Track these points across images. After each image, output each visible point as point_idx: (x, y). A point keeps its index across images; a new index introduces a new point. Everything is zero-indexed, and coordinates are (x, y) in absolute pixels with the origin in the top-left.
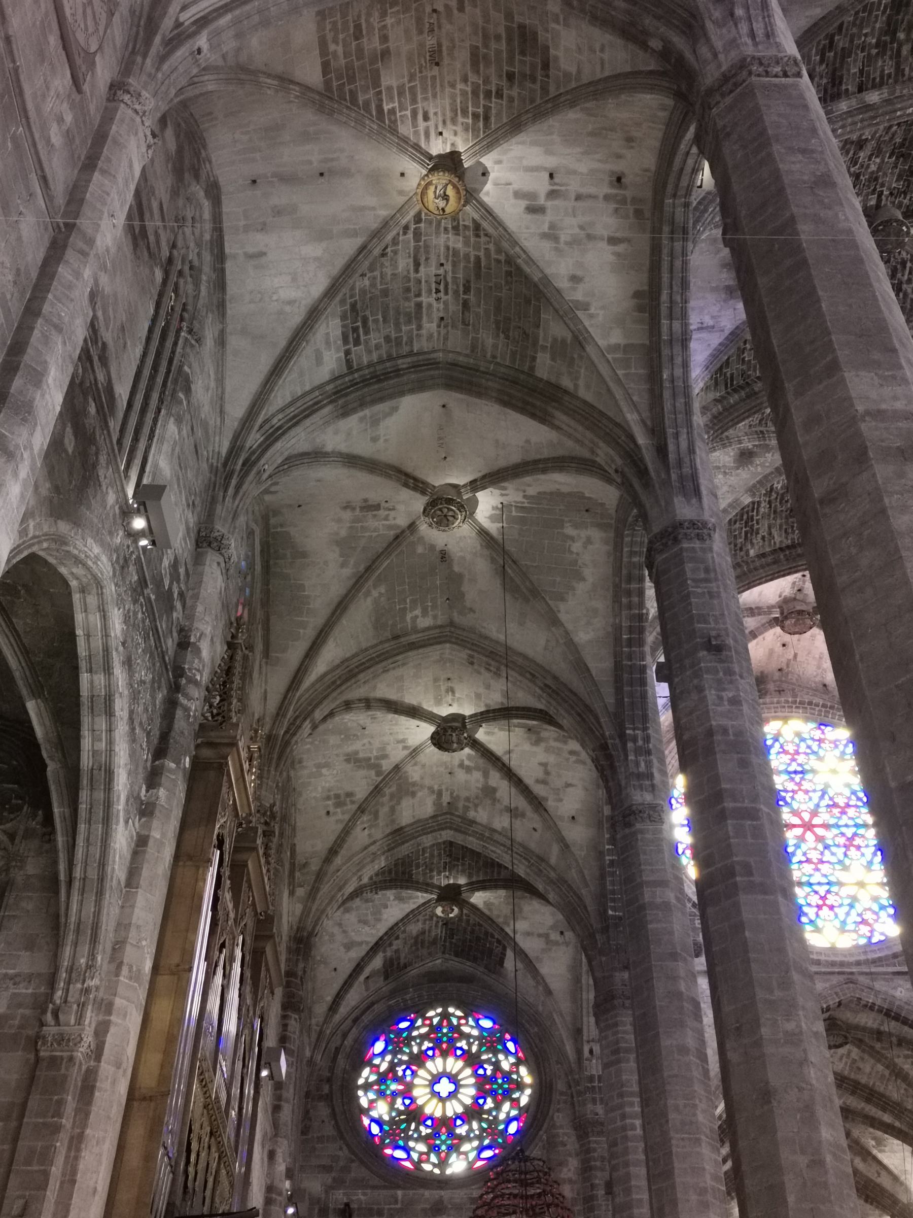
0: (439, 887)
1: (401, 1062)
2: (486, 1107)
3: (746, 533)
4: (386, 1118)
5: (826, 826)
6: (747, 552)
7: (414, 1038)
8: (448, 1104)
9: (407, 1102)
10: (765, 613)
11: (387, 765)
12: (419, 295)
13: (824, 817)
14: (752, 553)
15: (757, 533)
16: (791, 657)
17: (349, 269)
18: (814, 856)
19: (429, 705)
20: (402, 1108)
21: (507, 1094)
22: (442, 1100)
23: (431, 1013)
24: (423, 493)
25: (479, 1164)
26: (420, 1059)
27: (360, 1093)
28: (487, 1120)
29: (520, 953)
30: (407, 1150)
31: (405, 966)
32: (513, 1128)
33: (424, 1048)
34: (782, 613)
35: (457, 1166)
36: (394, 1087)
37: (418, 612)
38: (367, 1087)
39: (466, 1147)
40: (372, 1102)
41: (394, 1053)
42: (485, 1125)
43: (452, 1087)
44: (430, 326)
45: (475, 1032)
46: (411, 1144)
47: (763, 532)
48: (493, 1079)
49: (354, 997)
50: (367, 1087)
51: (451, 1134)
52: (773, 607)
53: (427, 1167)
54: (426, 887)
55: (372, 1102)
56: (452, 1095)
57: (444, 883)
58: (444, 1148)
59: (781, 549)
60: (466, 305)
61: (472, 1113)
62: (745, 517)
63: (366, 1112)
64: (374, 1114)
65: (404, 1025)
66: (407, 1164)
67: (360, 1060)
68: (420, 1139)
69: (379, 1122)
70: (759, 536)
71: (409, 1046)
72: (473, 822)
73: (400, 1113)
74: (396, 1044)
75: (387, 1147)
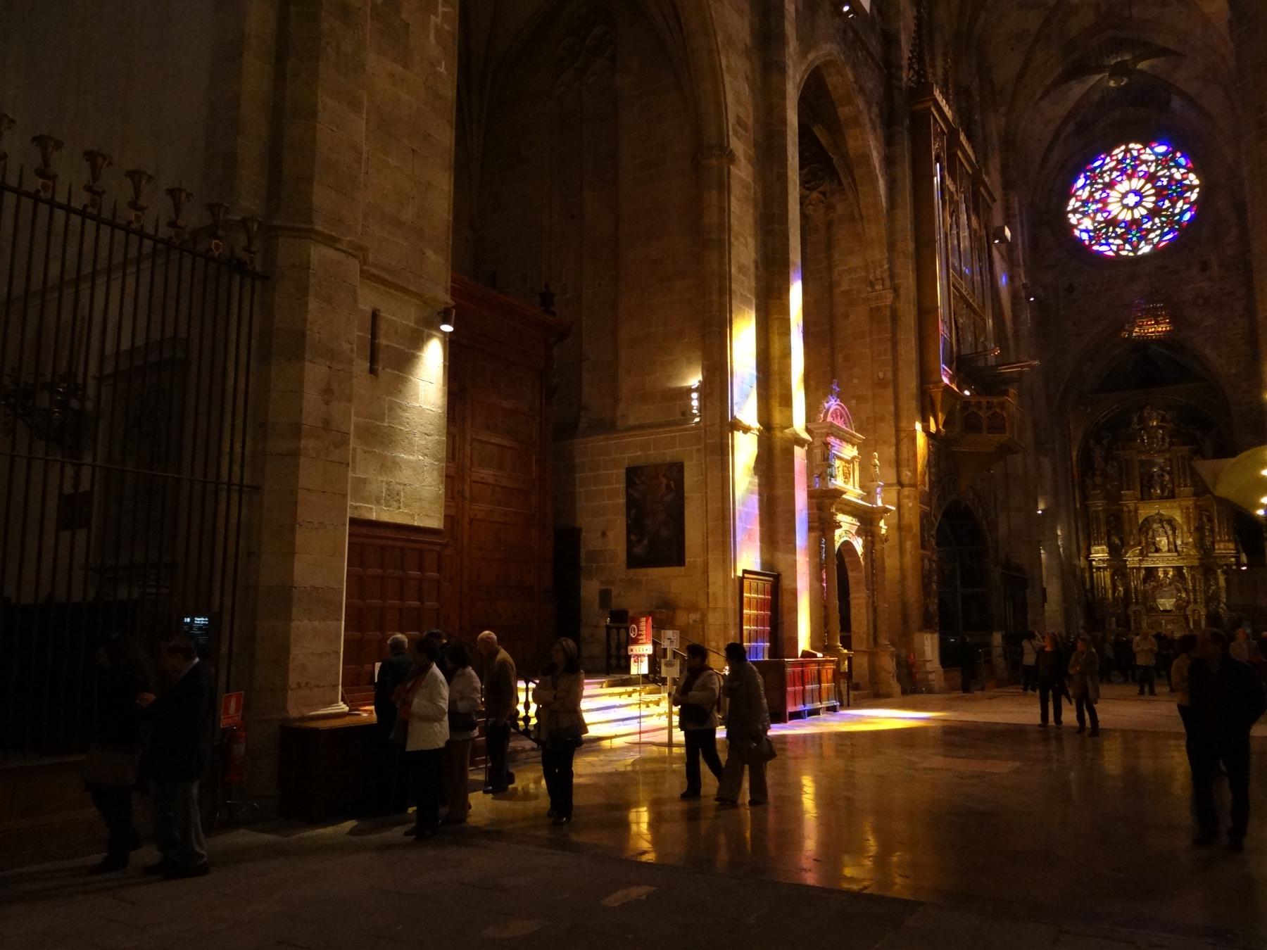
2: (1164, 207)
4: (1091, 228)
7: (1105, 172)
8: (1135, 211)
9: (1105, 215)
20: (1102, 219)
21: (1181, 196)
22: (1132, 209)
23: (1116, 151)
26: (1111, 185)
28: (1164, 216)
30: (1108, 244)
32: (1187, 216)
35: (1145, 249)
36: (1094, 207)
38: (1075, 211)
40: (1078, 220)
41: (1092, 185)
43: (1138, 198)
46: (1111, 241)
48: (1168, 187)
50: (1075, 211)
51: (1140, 229)
53: (1124, 253)
54: (1100, 69)
55: (1078, 220)
56: (1137, 204)
57: (1113, 62)
58: (1134, 239)
61: (1153, 213)
63: (1075, 227)
64: (1082, 227)
66: (1111, 253)
67: (1069, 195)
68: (1117, 237)
69: (1087, 231)
71: (1102, 178)
73: (1100, 223)
74: (1092, 180)
75: (1094, 245)
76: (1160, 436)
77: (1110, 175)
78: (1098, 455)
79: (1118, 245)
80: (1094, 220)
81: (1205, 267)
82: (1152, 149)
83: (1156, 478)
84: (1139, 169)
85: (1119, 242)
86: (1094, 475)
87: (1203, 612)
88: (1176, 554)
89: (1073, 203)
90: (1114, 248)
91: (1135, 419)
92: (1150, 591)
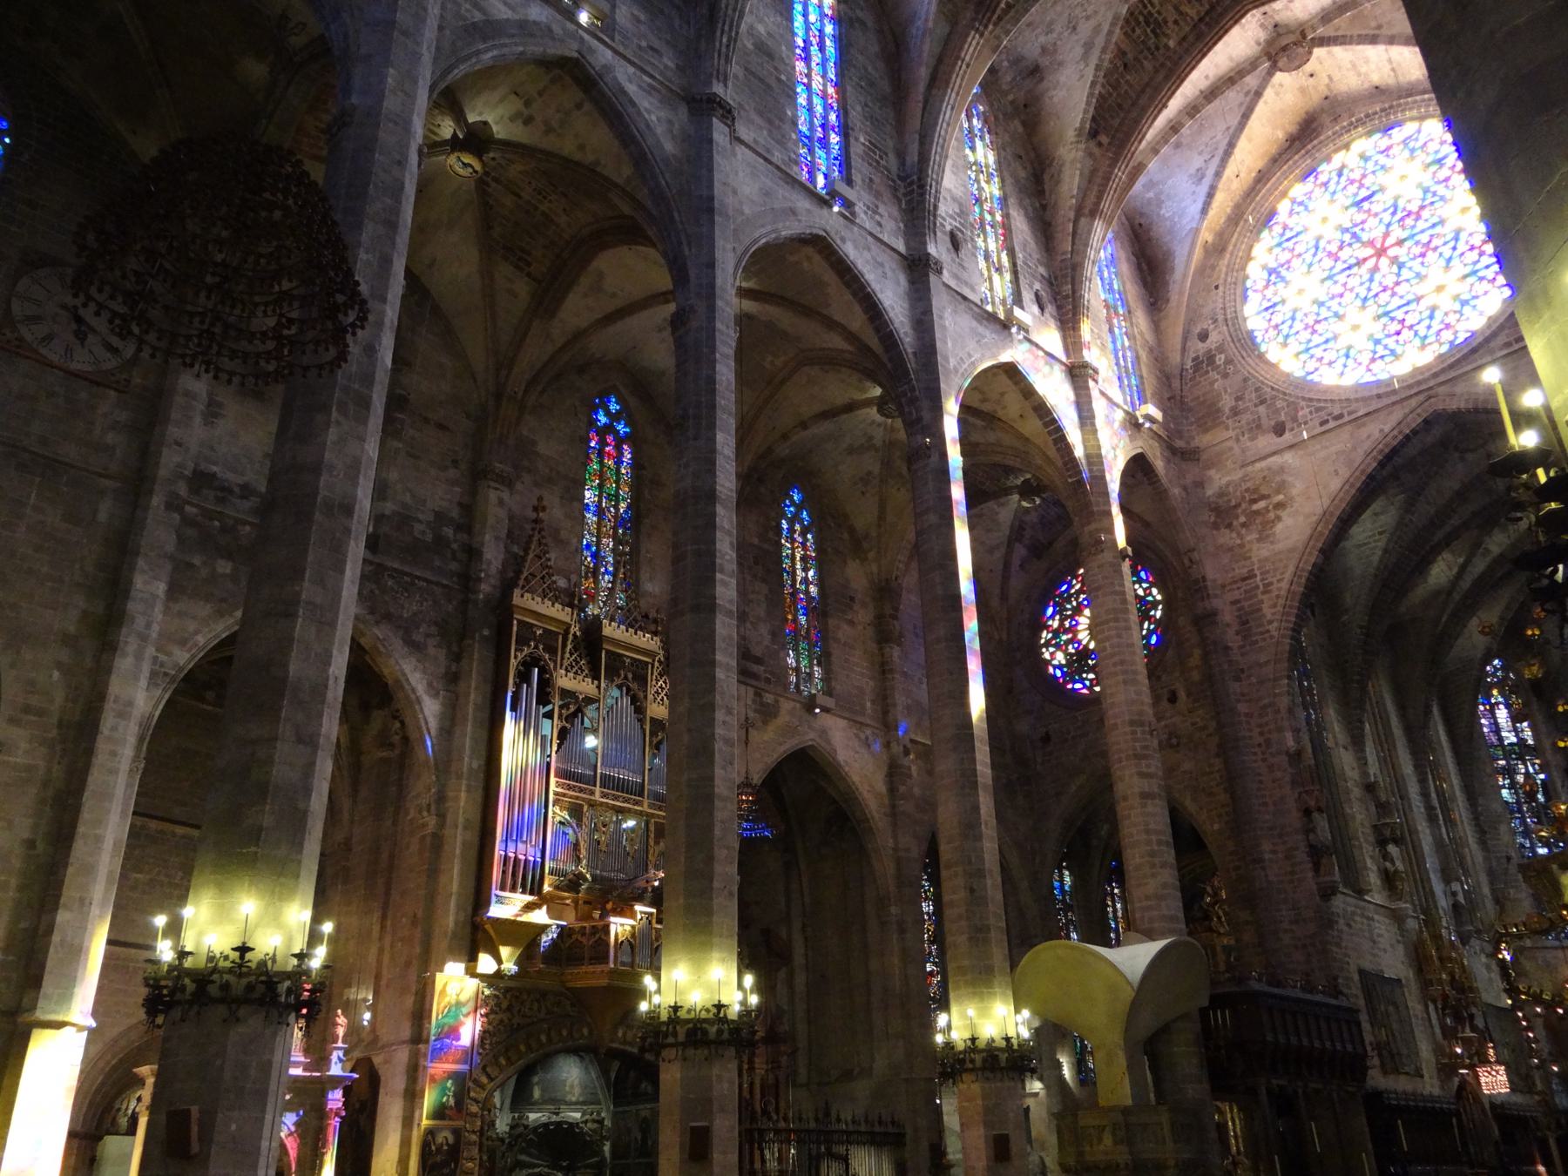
3: (1153, 31)
4: (1064, 662)
5: (1400, 243)
6: (1166, 46)
10: (1249, 72)
11: (878, 442)
12: (536, 208)
13: (1397, 233)
14: (1172, 44)
15: (1166, 22)
16: (1326, 81)
18: (1390, 281)
30: (1082, 681)
31: (1050, 544)
34: (1269, 59)
36: (1064, 637)
41: (1060, 613)
47: (1171, 16)
50: (1048, 644)
52: (1257, 59)
59: (1201, 20)
62: (1141, 19)
64: (1055, 662)
66: (1085, 691)
69: (1060, 667)
70: (1170, 24)
71: (1070, 603)
73: (1071, 655)
75: (1068, 683)
77: (1076, 599)
79: (1091, 680)
80: (1066, 654)
85: (1091, 676)
90: (1087, 683)
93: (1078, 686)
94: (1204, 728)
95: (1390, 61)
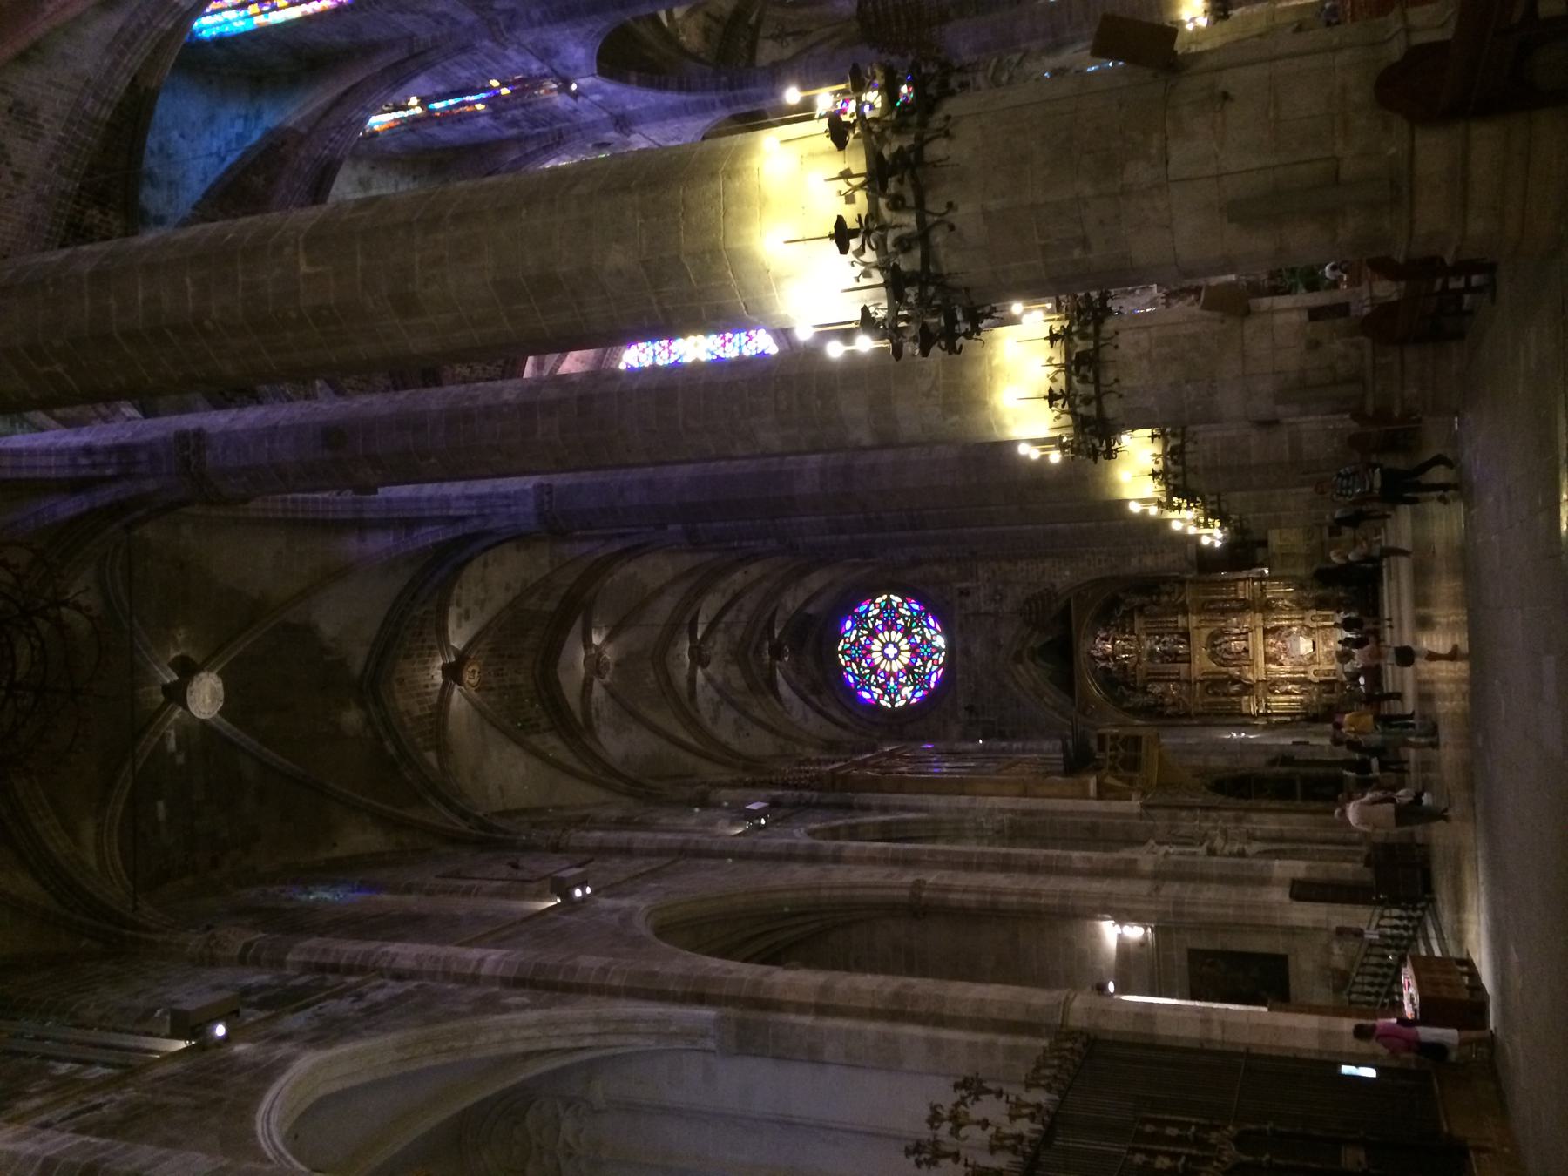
0: (771, 659)
1: (876, 680)
4: (912, 687)
7: (860, 672)
8: (902, 648)
9: (901, 674)
11: (717, 698)
17: (504, 731)
19: (686, 671)
21: (896, 610)
22: (899, 651)
23: (843, 662)
24: (592, 680)
25: (938, 628)
26: (874, 669)
27: (896, 705)
28: (911, 624)
29: (807, 602)
30: (931, 674)
32: (916, 607)
33: (866, 665)
35: (940, 642)
36: (892, 684)
37: (647, 680)
38: (893, 701)
39: (928, 636)
40: (902, 698)
42: (914, 624)
43: (891, 646)
44: (520, 679)
45: (855, 632)
46: (927, 671)
49: (836, 713)
50: (893, 701)
54: (772, 668)
56: (896, 645)
57: (768, 657)
58: (929, 650)
60: (510, 656)
61: (907, 633)
64: (909, 696)
65: (851, 679)
66: (940, 672)
67: (875, 707)
68: (924, 665)
69: (914, 692)
72: (742, 638)
73: (908, 679)
74: (866, 685)
75: (929, 685)
76: (1123, 643)
78: (1140, 699)
80: (905, 685)
81: (965, 593)
82: (847, 631)
83: (1166, 648)
84: (863, 643)
86: (1162, 705)
87: (1314, 612)
88: (1250, 634)
89: (885, 703)
91: (1103, 664)
92: (1292, 660)
93: (934, 678)
94: (994, 572)
95: (577, 360)
